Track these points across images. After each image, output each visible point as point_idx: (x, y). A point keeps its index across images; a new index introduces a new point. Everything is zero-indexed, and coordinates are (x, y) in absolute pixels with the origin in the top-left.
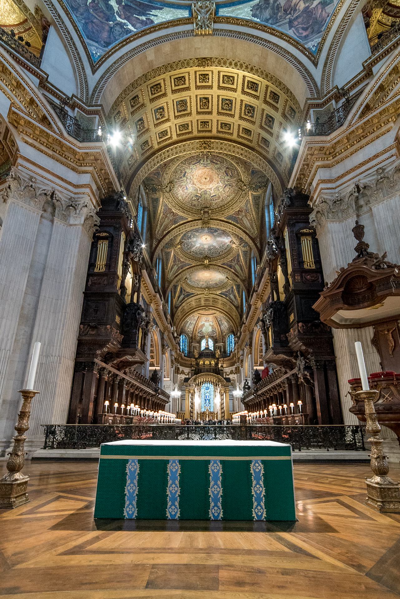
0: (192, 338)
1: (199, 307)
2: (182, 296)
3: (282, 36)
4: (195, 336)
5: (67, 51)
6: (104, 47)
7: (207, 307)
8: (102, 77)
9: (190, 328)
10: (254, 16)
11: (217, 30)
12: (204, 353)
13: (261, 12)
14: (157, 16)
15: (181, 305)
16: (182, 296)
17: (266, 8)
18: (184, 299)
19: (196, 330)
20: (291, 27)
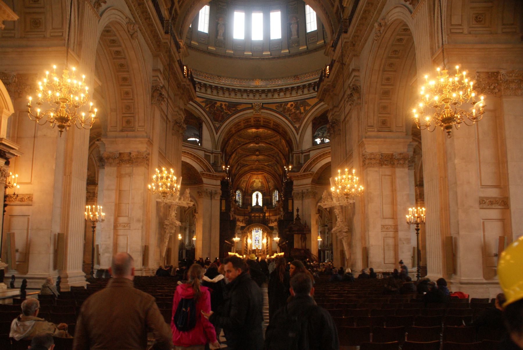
0: (245, 192)
1: (251, 170)
2: (239, 167)
3: (287, 119)
4: (248, 190)
5: (209, 131)
7: (257, 170)
8: (220, 135)
9: (243, 185)
10: (277, 109)
11: (262, 112)
12: (255, 208)
13: (279, 108)
15: (238, 173)
16: (239, 167)
17: (281, 107)
18: (240, 168)
19: (248, 186)
20: (290, 116)
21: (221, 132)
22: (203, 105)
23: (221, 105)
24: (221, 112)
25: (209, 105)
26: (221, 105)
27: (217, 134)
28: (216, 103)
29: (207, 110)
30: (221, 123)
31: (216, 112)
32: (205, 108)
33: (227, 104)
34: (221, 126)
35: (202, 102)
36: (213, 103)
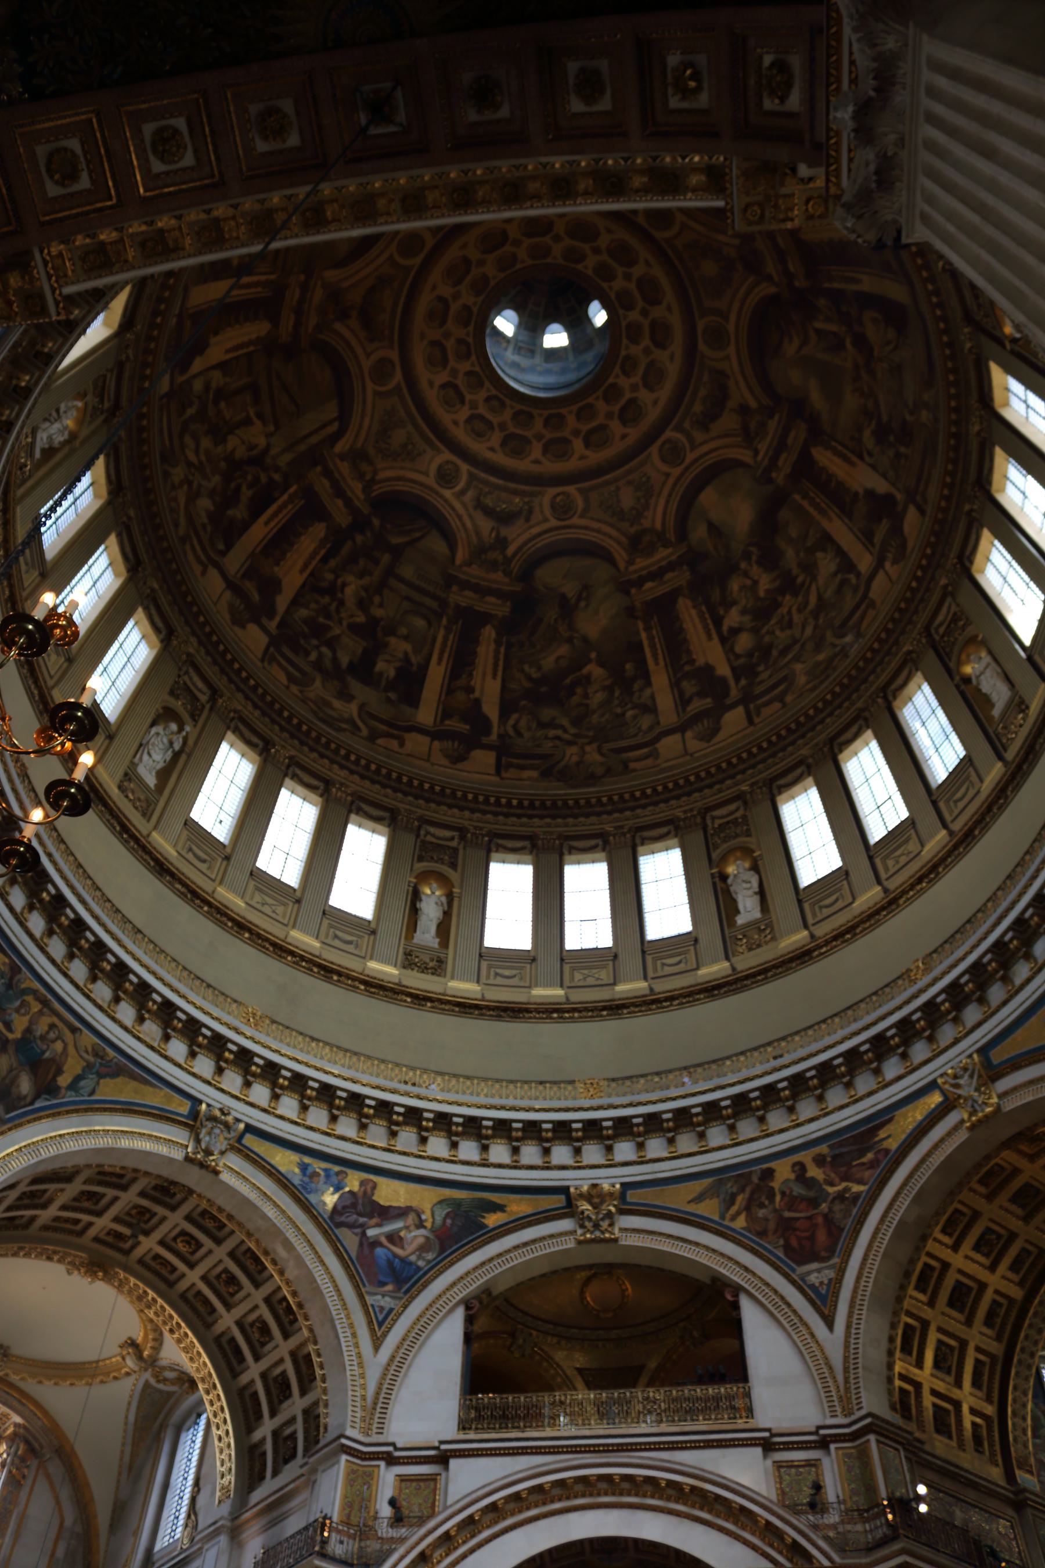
6: (828, 1258)
14: (889, 1136)
21: (852, 1305)
22: (709, 1209)
23: (800, 1169)
24: (814, 1203)
25: (740, 1200)
26: (800, 1169)
27: (829, 1322)
28: (769, 1174)
29: (741, 1222)
30: (836, 1260)
31: (787, 1214)
32: (726, 1223)
33: (823, 1149)
34: (841, 1271)
35: (699, 1199)
36: (755, 1179)
